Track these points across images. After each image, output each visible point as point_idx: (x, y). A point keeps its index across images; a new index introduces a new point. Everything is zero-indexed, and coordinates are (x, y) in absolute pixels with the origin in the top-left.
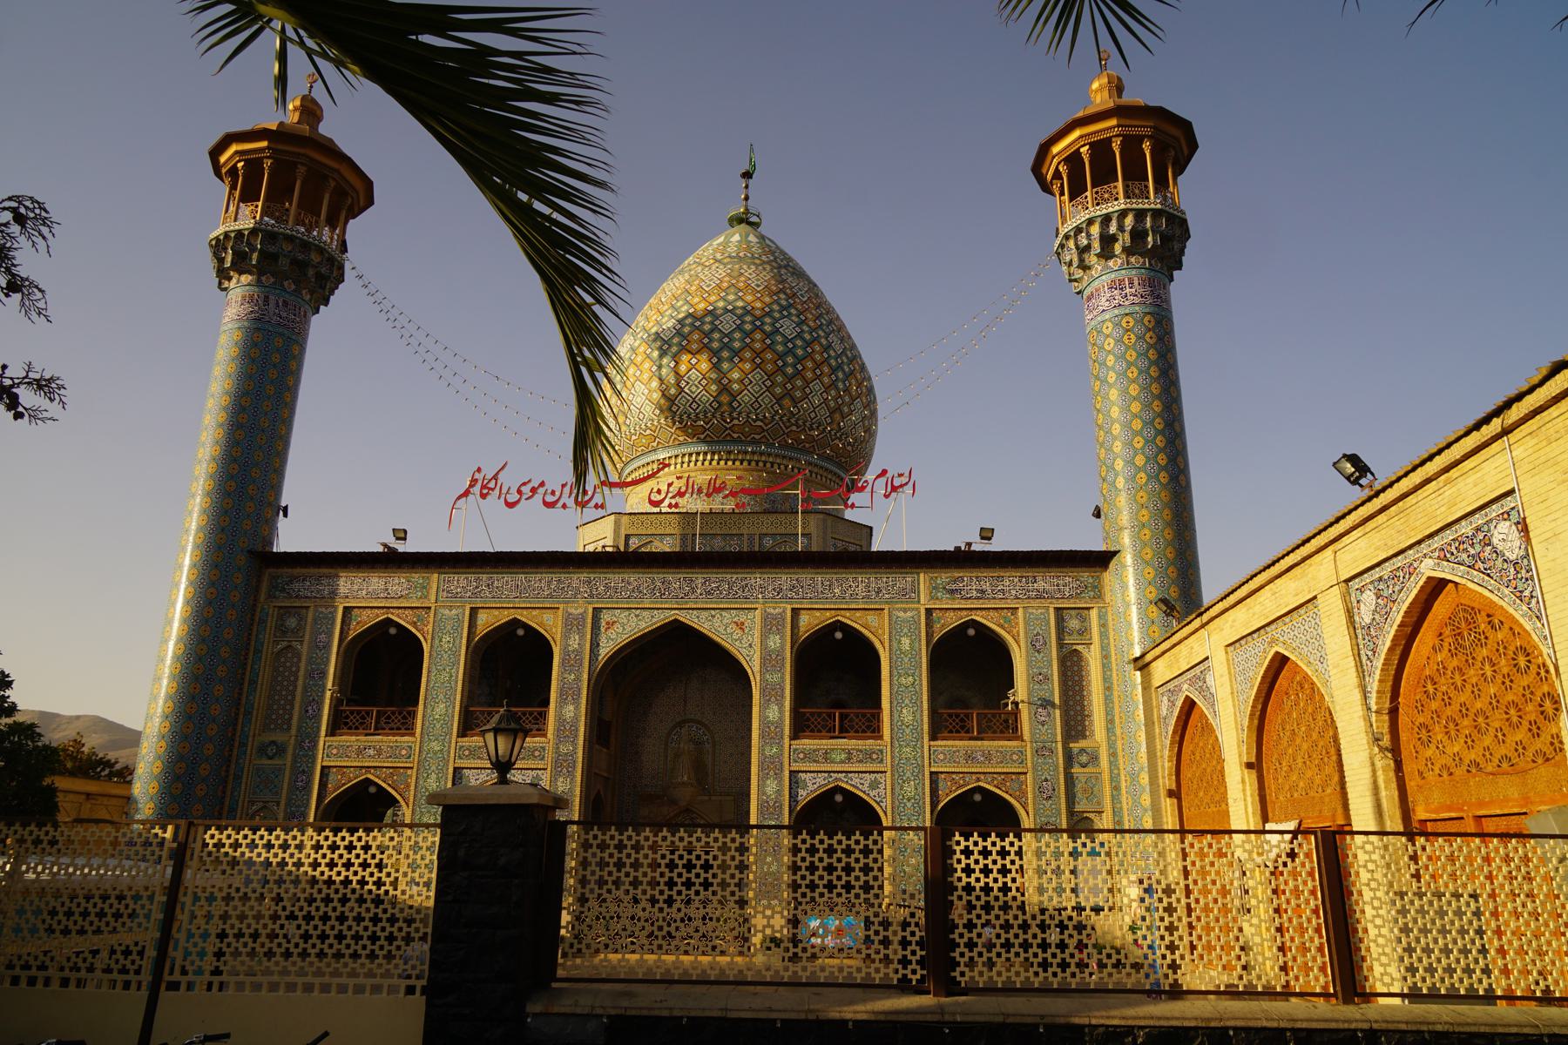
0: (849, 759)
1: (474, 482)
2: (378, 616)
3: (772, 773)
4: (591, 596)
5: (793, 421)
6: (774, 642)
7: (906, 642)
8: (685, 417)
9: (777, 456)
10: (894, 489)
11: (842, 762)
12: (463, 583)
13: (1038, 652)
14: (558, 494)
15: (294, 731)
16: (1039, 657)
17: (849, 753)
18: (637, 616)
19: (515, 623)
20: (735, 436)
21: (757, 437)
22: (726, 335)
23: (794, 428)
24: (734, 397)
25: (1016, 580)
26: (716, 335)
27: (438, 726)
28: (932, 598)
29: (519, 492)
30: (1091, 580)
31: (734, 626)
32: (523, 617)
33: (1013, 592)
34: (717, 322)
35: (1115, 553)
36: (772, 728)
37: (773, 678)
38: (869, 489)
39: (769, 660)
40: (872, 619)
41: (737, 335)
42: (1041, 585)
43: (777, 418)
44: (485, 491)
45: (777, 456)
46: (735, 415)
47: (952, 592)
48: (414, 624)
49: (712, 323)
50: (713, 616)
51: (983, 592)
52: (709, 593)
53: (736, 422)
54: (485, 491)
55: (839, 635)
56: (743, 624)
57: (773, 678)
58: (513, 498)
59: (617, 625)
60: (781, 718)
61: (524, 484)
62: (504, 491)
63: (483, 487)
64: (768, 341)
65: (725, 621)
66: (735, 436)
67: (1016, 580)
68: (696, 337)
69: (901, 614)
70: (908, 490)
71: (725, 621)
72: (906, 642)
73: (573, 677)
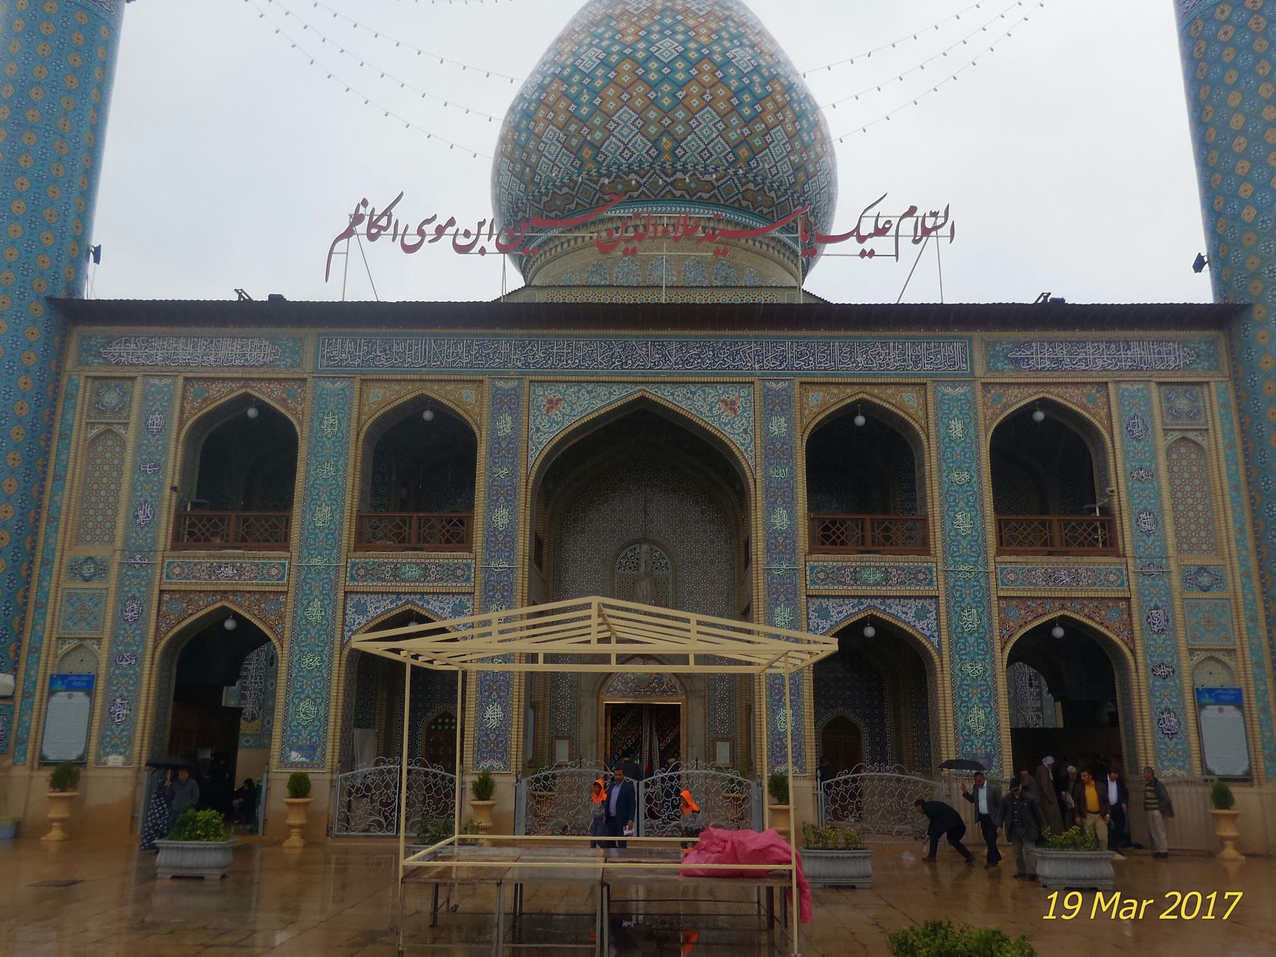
0: (887, 580)
1: (357, 218)
2: (232, 391)
3: (782, 598)
4: (527, 365)
5: (750, 176)
6: (778, 426)
8: (614, 169)
10: (927, 232)
11: (877, 584)
12: (349, 346)
13: (1137, 439)
14: (473, 238)
15: (119, 543)
16: (1139, 446)
17: (886, 572)
18: (589, 392)
19: (423, 402)
20: (678, 193)
21: (706, 196)
22: (666, 65)
23: (751, 186)
24: (678, 142)
25: (1103, 346)
26: (653, 65)
27: (321, 536)
29: (421, 232)
30: (1204, 347)
31: (723, 407)
32: (435, 392)
33: (1099, 362)
34: (653, 49)
35: (1250, 305)
36: (781, 539)
37: (780, 473)
38: (892, 231)
39: (775, 451)
41: (680, 65)
42: (1136, 352)
44: (374, 231)
46: (678, 165)
48: (283, 401)
49: (647, 50)
51: (1058, 361)
53: (679, 175)
54: (374, 231)
55: (860, 420)
56: (733, 403)
57: (780, 473)
58: (412, 240)
59: (560, 406)
60: (792, 527)
61: (427, 221)
62: (401, 231)
63: (372, 224)
64: (719, 74)
65: (709, 400)
68: (627, 66)
70: (945, 230)
71: (709, 400)
73: (505, 471)
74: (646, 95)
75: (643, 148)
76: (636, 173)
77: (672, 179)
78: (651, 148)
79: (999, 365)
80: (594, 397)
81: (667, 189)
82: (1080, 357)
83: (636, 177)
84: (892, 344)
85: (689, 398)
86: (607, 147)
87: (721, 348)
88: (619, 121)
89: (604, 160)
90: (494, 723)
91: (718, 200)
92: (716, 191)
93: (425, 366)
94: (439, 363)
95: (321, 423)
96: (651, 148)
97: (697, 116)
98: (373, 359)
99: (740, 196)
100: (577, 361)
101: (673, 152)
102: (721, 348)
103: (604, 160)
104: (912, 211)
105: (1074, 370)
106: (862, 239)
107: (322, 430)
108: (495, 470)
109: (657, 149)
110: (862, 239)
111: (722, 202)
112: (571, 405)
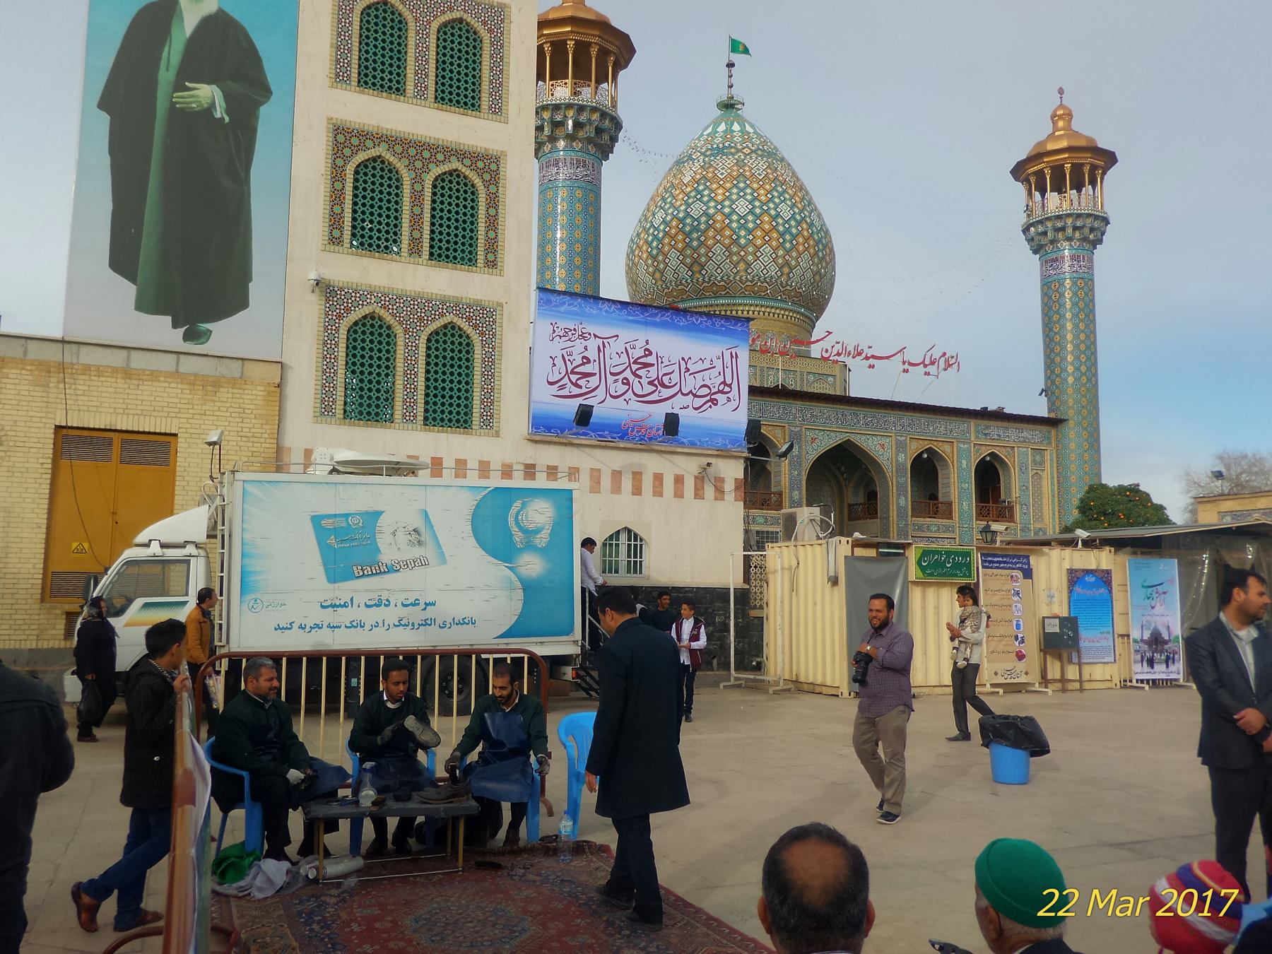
4: (803, 420)
7: (964, 462)
9: (791, 310)
10: (950, 365)
11: (935, 532)
28: (977, 437)
37: (902, 480)
39: (900, 469)
40: (947, 448)
42: (1025, 434)
45: (791, 310)
51: (999, 436)
53: (788, 288)
57: (902, 480)
60: (907, 505)
69: (962, 446)
70: (955, 366)
72: (964, 462)
104: (945, 354)
106: (926, 366)
110: (926, 366)
112: (821, 441)
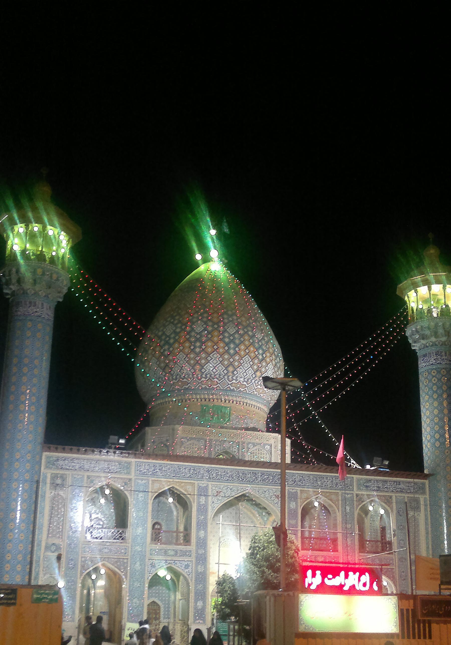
7: (348, 508)
8: (208, 376)
13: (401, 516)
18: (231, 489)
23: (259, 387)
25: (392, 483)
33: (391, 489)
43: (253, 381)
46: (234, 378)
47: (367, 487)
50: (265, 492)
51: (379, 487)
52: (263, 480)
53: (234, 381)
57: (293, 522)
66: (232, 388)
67: (392, 483)
71: (271, 494)
72: (348, 508)
73: (203, 517)
74: (224, 348)
75: (222, 369)
76: (217, 378)
77: (231, 382)
78: (224, 370)
79: (361, 487)
80: (232, 491)
81: (228, 386)
82: (385, 486)
83: (217, 380)
84: (329, 478)
85: (263, 494)
86: (206, 367)
87: (275, 476)
88: (213, 357)
89: (205, 372)
90: (200, 607)
91: (247, 392)
92: (246, 388)
93: (174, 476)
94: (179, 475)
95: (138, 496)
96: (224, 370)
97: (243, 359)
98: (156, 472)
99: (254, 390)
100: (227, 478)
101: (233, 372)
102: (275, 476)
103: (205, 372)
105: (384, 491)
107: (138, 499)
108: (200, 516)
109: (227, 371)
111: (248, 392)
